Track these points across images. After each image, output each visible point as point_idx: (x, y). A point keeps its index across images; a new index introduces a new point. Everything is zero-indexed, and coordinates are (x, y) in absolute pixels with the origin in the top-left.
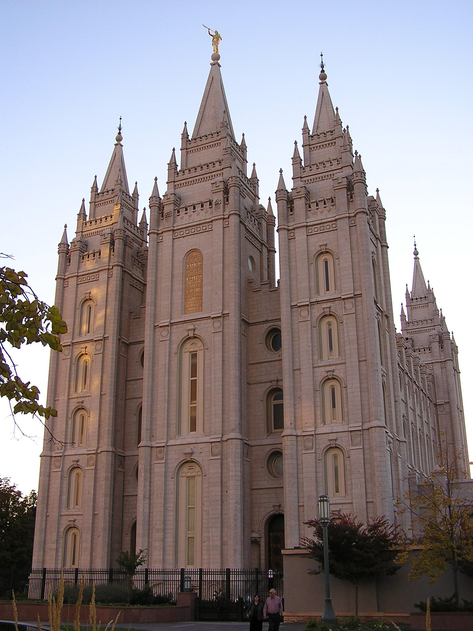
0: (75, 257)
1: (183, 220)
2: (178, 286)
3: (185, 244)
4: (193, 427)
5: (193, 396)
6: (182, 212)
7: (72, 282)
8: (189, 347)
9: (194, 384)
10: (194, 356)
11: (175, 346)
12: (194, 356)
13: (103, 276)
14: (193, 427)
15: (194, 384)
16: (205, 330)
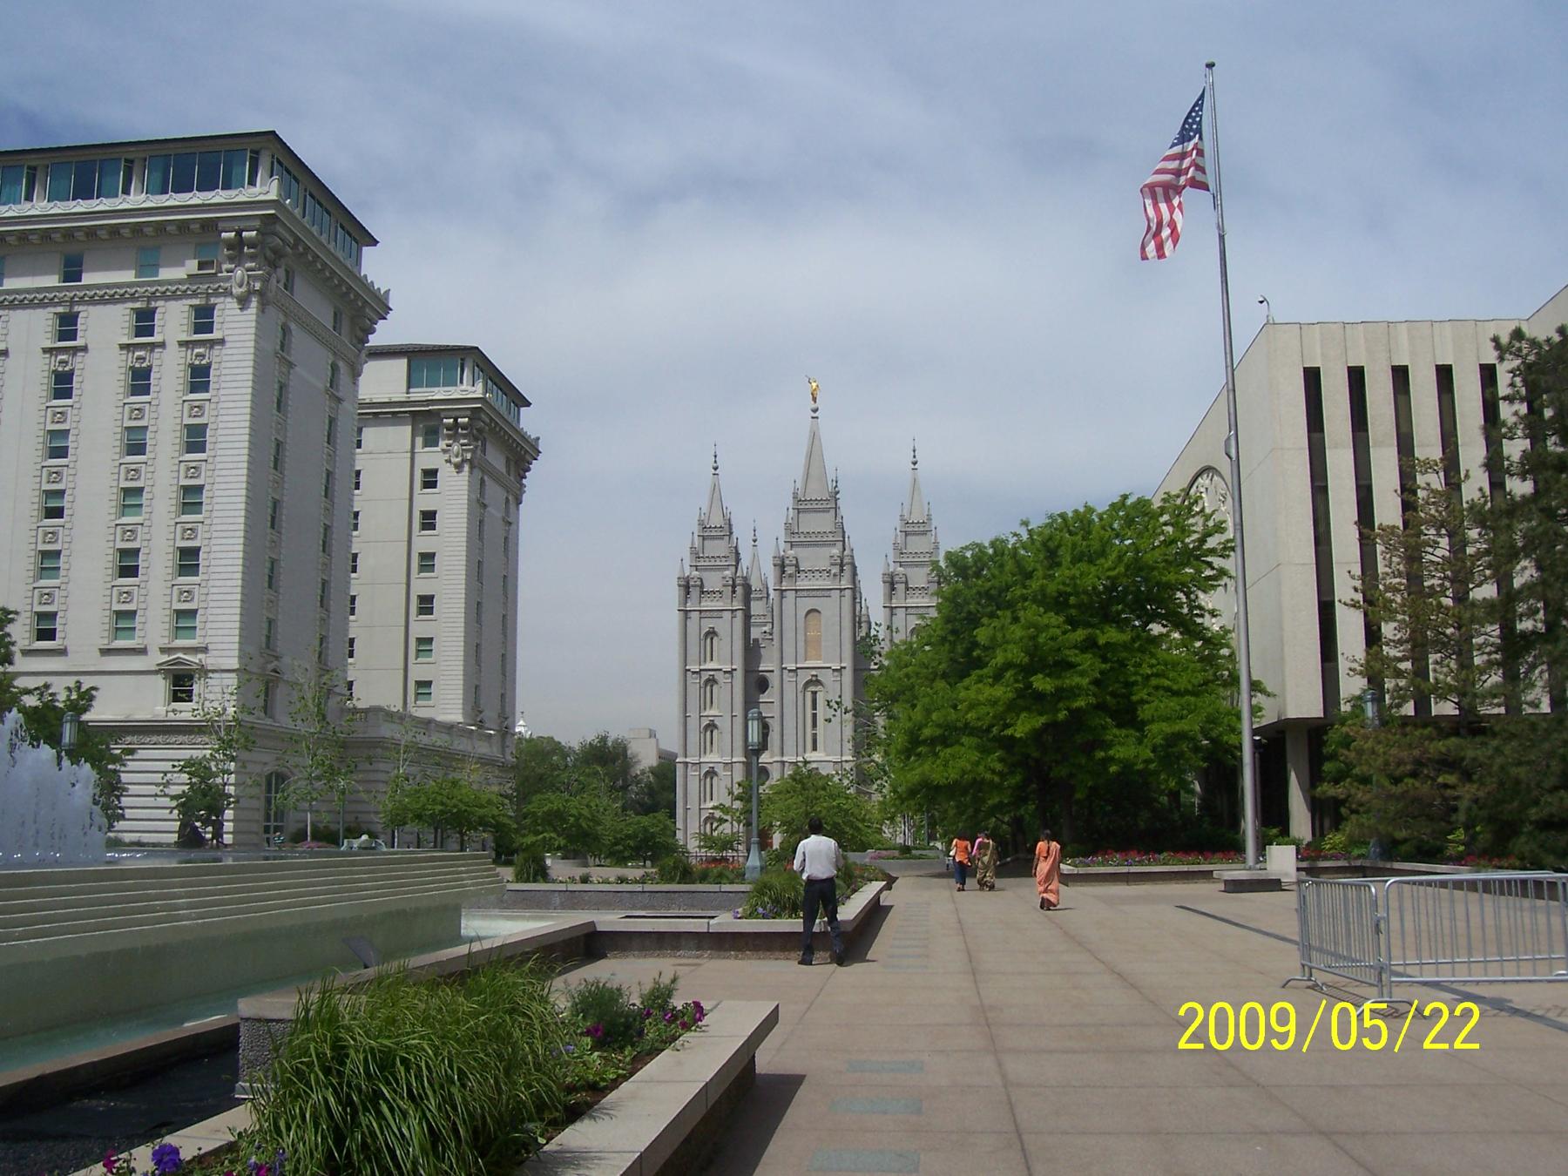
0: (695, 593)
1: (802, 584)
2: (801, 638)
3: (807, 604)
4: (815, 748)
5: (814, 725)
6: (803, 575)
7: (695, 616)
8: (813, 689)
9: (814, 716)
10: (814, 693)
11: (800, 686)
12: (814, 693)
13: (727, 615)
14: (815, 748)
15: (814, 716)
16: (827, 678)
